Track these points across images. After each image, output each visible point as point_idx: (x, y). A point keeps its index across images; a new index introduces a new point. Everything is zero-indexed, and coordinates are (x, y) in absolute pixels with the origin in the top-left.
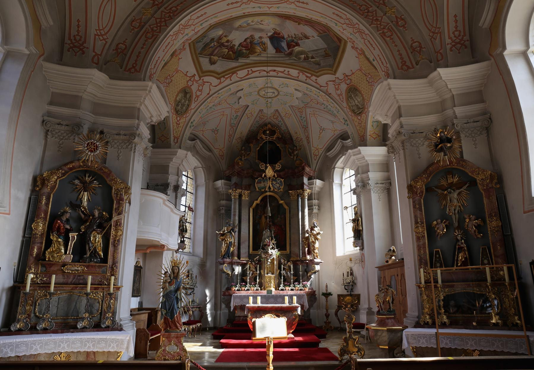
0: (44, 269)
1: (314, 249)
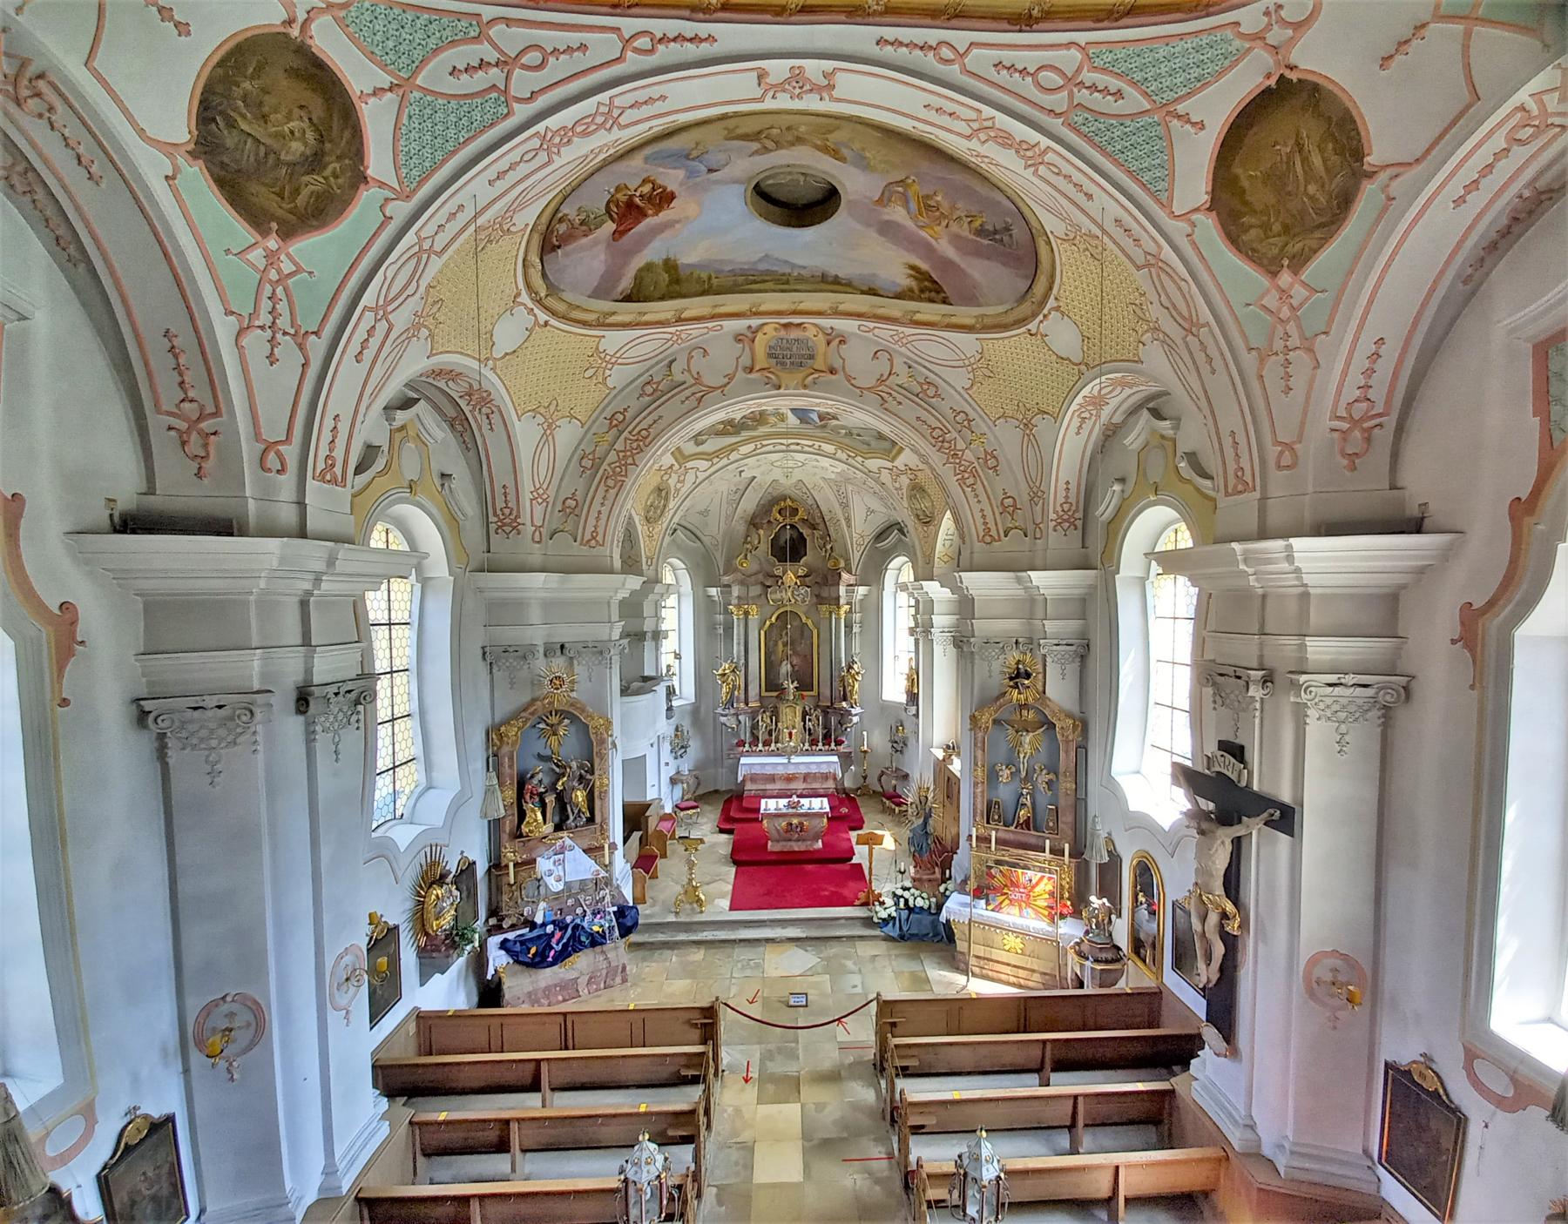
1: (852, 695)
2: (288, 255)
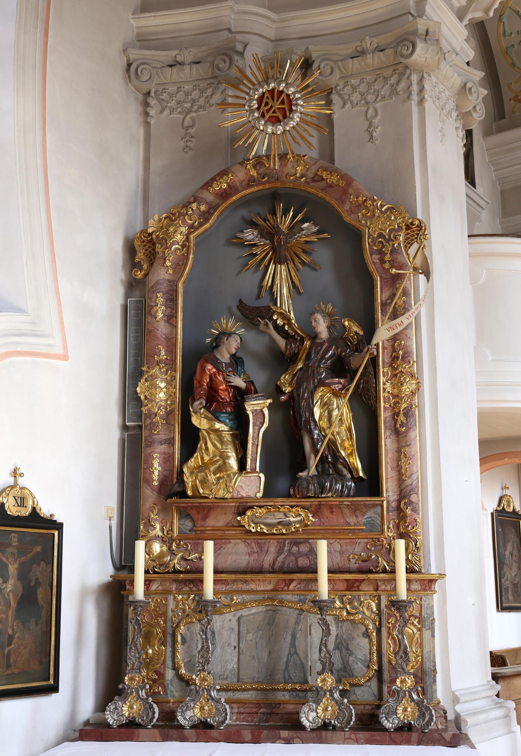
0: (189, 524)
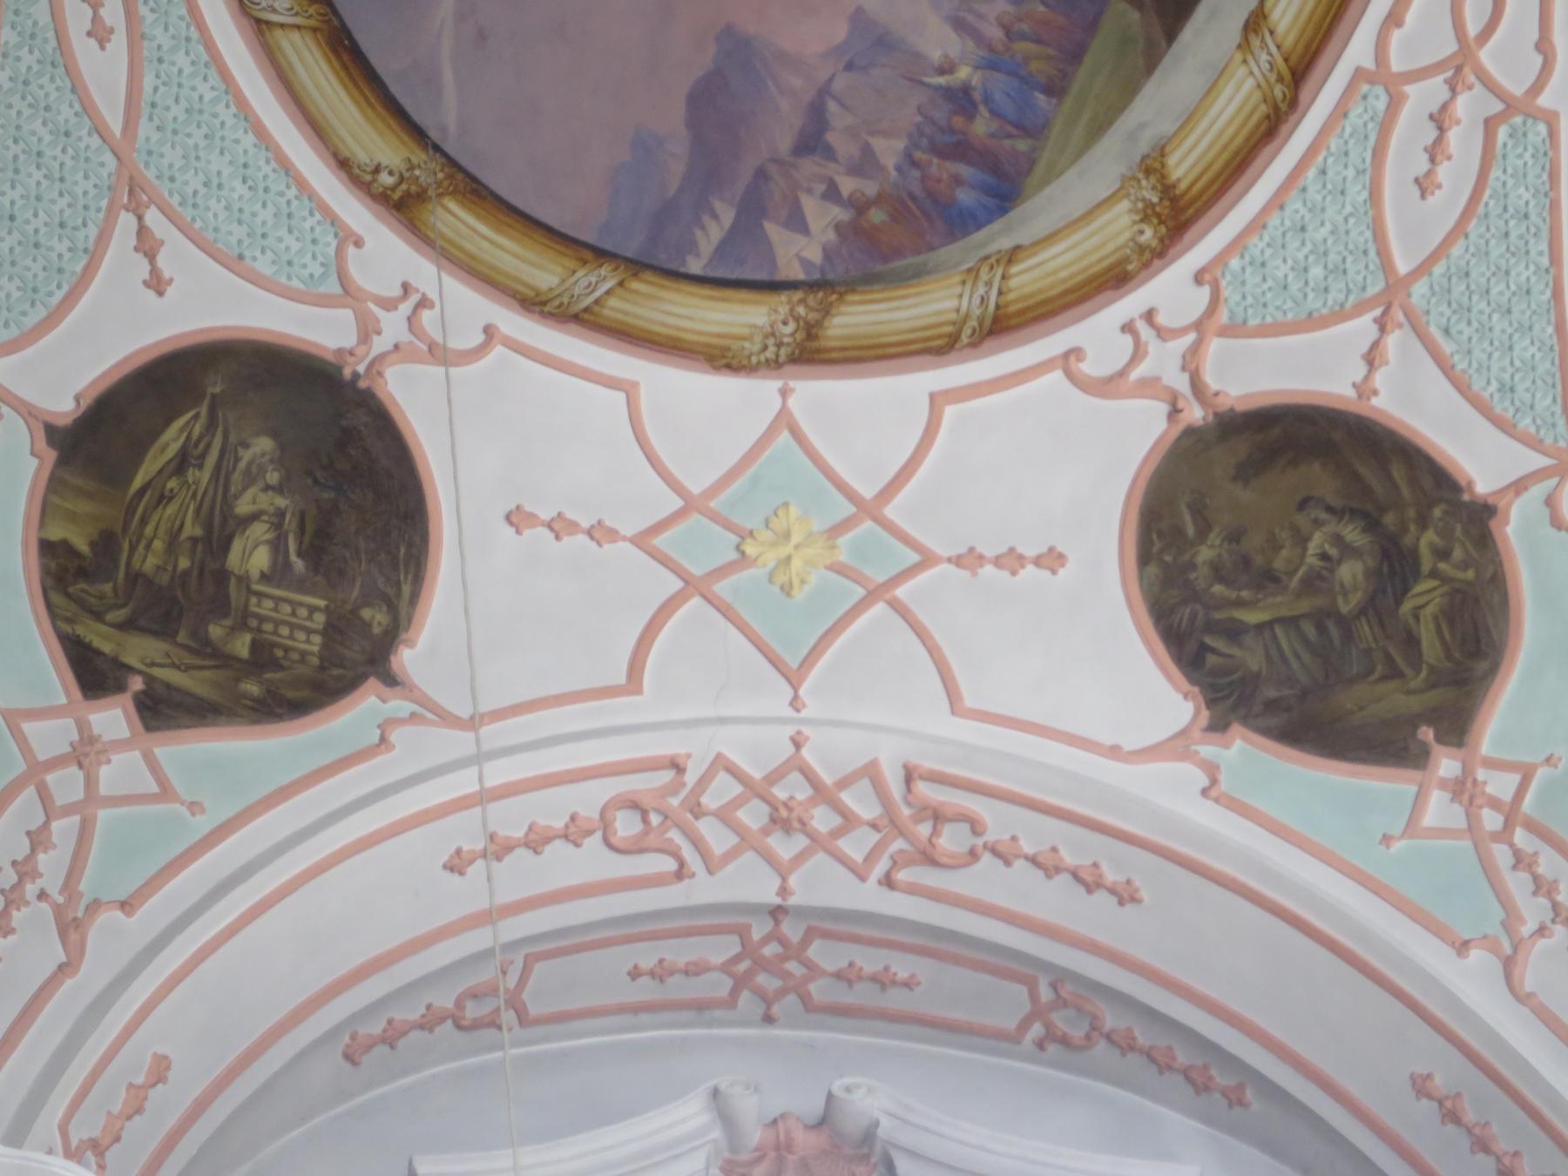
2: (1491, 764)
